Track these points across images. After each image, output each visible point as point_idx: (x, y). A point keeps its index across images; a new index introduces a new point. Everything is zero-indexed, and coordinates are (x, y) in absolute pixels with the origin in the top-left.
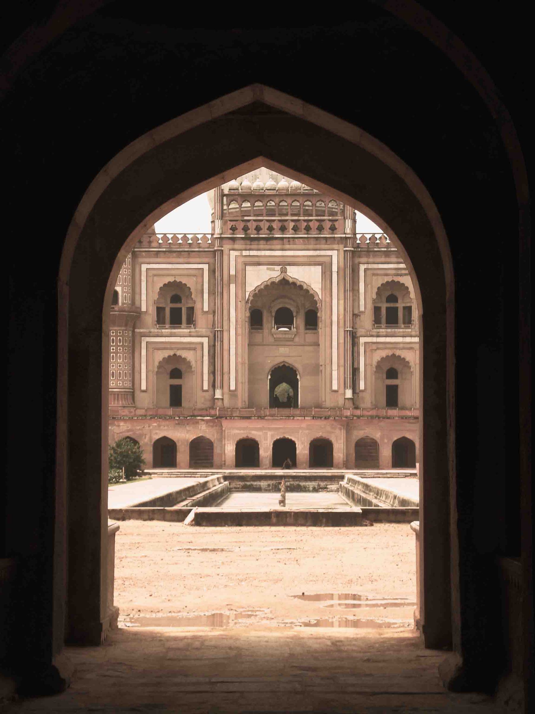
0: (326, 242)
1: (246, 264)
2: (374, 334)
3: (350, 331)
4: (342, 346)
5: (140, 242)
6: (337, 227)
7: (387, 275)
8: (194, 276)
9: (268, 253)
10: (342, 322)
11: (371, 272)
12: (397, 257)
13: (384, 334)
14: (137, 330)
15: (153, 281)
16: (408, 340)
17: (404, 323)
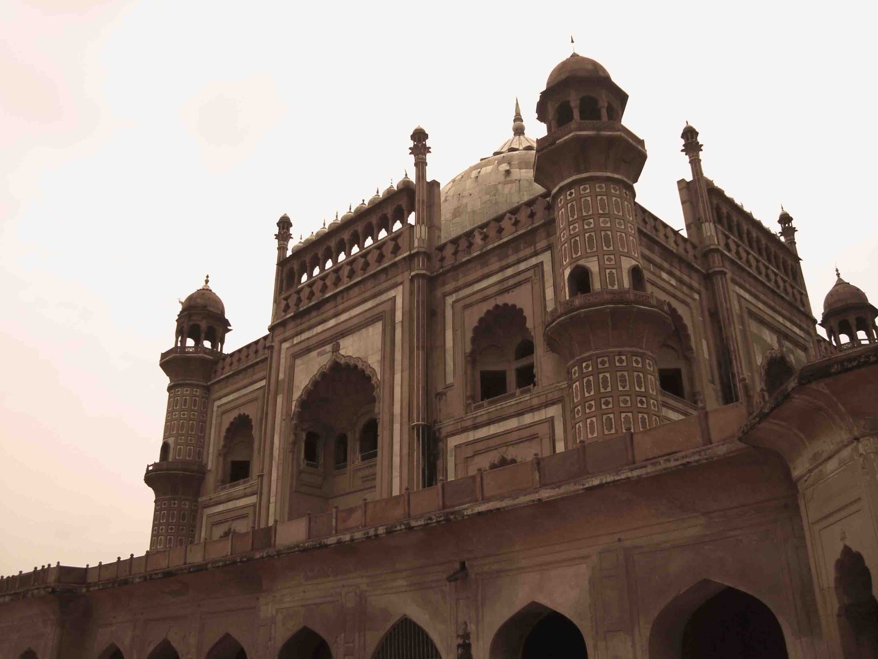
0: (387, 275)
1: (295, 356)
2: (469, 423)
3: (418, 426)
4: (406, 458)
5: (216, 372)
6: (400, 245)
7: (485, 299)
8: (256, 399)
9: (319, 329)
10: (406, 414)
11: (462, 303)
12: (500, 260)
13: (485, 418)
14: (200, 500)
15: (220, 424)
16: (528, 419)
17: (520, 385)
